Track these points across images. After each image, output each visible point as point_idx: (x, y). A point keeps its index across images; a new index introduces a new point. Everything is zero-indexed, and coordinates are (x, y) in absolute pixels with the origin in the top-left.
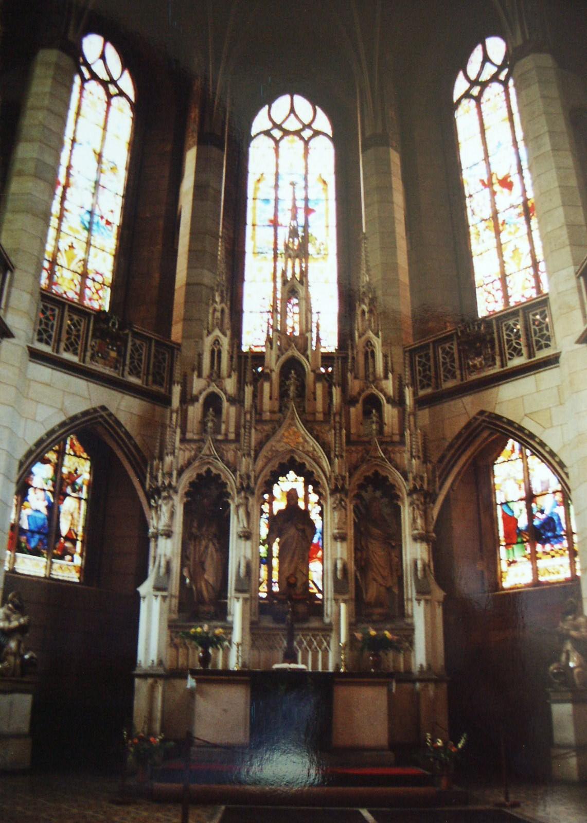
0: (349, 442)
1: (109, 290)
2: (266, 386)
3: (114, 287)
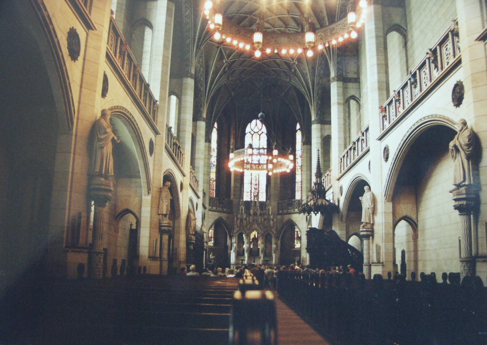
0: (264, 227)
1: (215, 182)
2: (251, 217)
3: (216, 181)
